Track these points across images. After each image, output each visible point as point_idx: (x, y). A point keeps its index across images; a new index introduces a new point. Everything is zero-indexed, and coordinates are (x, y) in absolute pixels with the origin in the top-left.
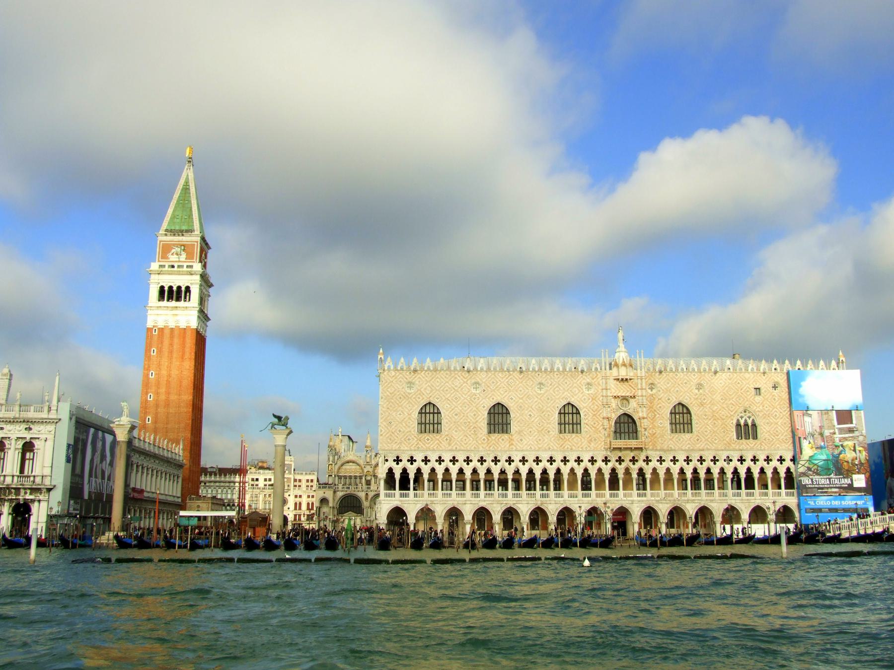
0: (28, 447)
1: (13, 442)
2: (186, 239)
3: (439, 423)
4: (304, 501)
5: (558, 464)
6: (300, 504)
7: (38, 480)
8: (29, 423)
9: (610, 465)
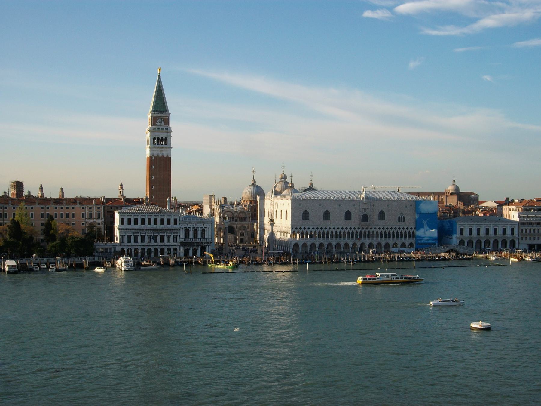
0: (203, 231)
2: (163, 115)
3: (309, 216)
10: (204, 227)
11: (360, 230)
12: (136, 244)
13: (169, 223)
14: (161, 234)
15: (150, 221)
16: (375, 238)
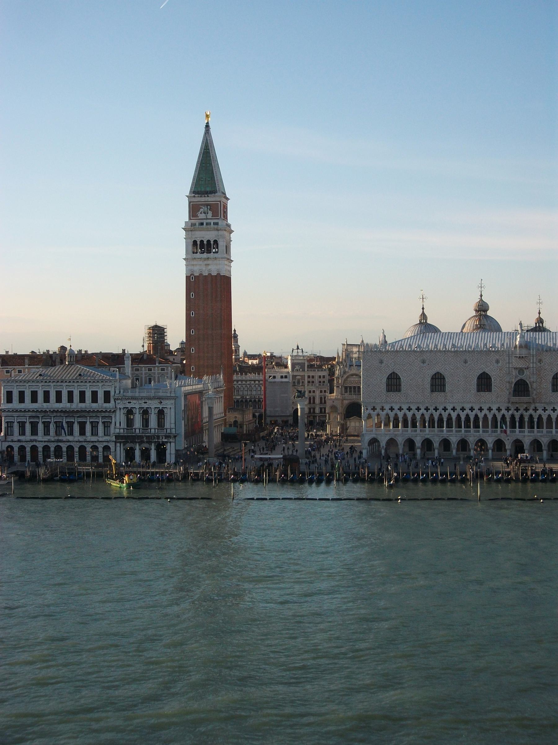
0: (161, 413)
1: (153, 410)
2: (211, 199)
3: (400, 385)
4: (317, 394)
5: (476, 411)
6: (314, 398)
7: (169, 431)
8: (160, 399)
9: (510, 412)
10: (161, 407)
11: (510, 412)
12: (33, 438)
13: (95, 398)
14: (80, 420)
15: (22, 395)
16: (545, 430)
